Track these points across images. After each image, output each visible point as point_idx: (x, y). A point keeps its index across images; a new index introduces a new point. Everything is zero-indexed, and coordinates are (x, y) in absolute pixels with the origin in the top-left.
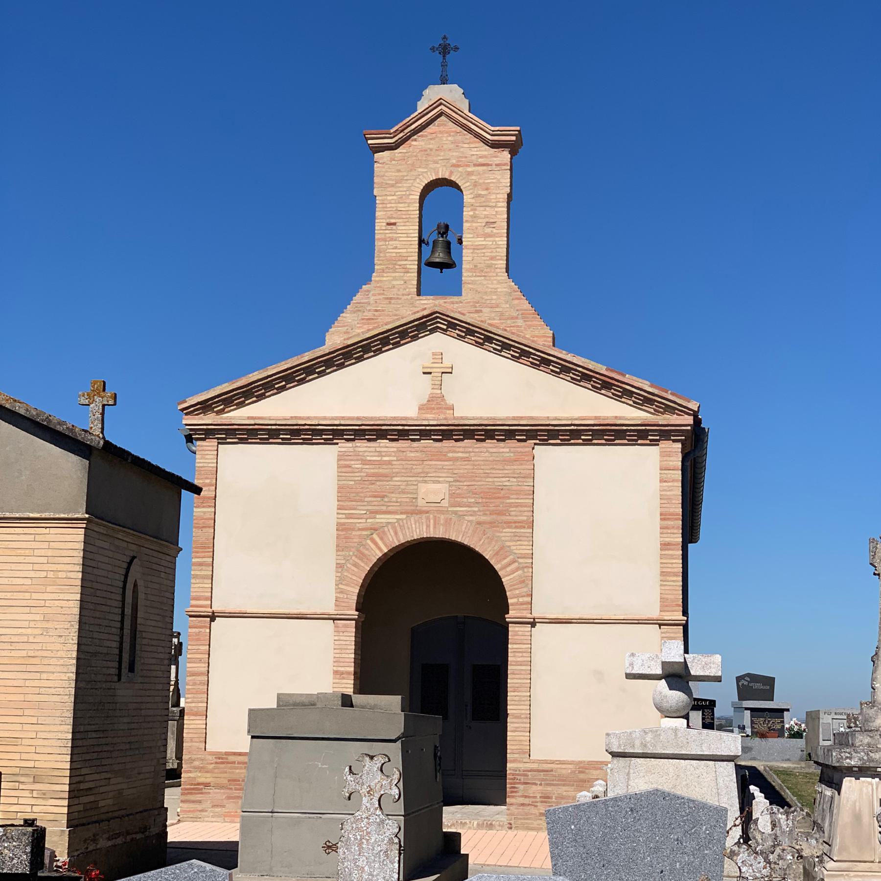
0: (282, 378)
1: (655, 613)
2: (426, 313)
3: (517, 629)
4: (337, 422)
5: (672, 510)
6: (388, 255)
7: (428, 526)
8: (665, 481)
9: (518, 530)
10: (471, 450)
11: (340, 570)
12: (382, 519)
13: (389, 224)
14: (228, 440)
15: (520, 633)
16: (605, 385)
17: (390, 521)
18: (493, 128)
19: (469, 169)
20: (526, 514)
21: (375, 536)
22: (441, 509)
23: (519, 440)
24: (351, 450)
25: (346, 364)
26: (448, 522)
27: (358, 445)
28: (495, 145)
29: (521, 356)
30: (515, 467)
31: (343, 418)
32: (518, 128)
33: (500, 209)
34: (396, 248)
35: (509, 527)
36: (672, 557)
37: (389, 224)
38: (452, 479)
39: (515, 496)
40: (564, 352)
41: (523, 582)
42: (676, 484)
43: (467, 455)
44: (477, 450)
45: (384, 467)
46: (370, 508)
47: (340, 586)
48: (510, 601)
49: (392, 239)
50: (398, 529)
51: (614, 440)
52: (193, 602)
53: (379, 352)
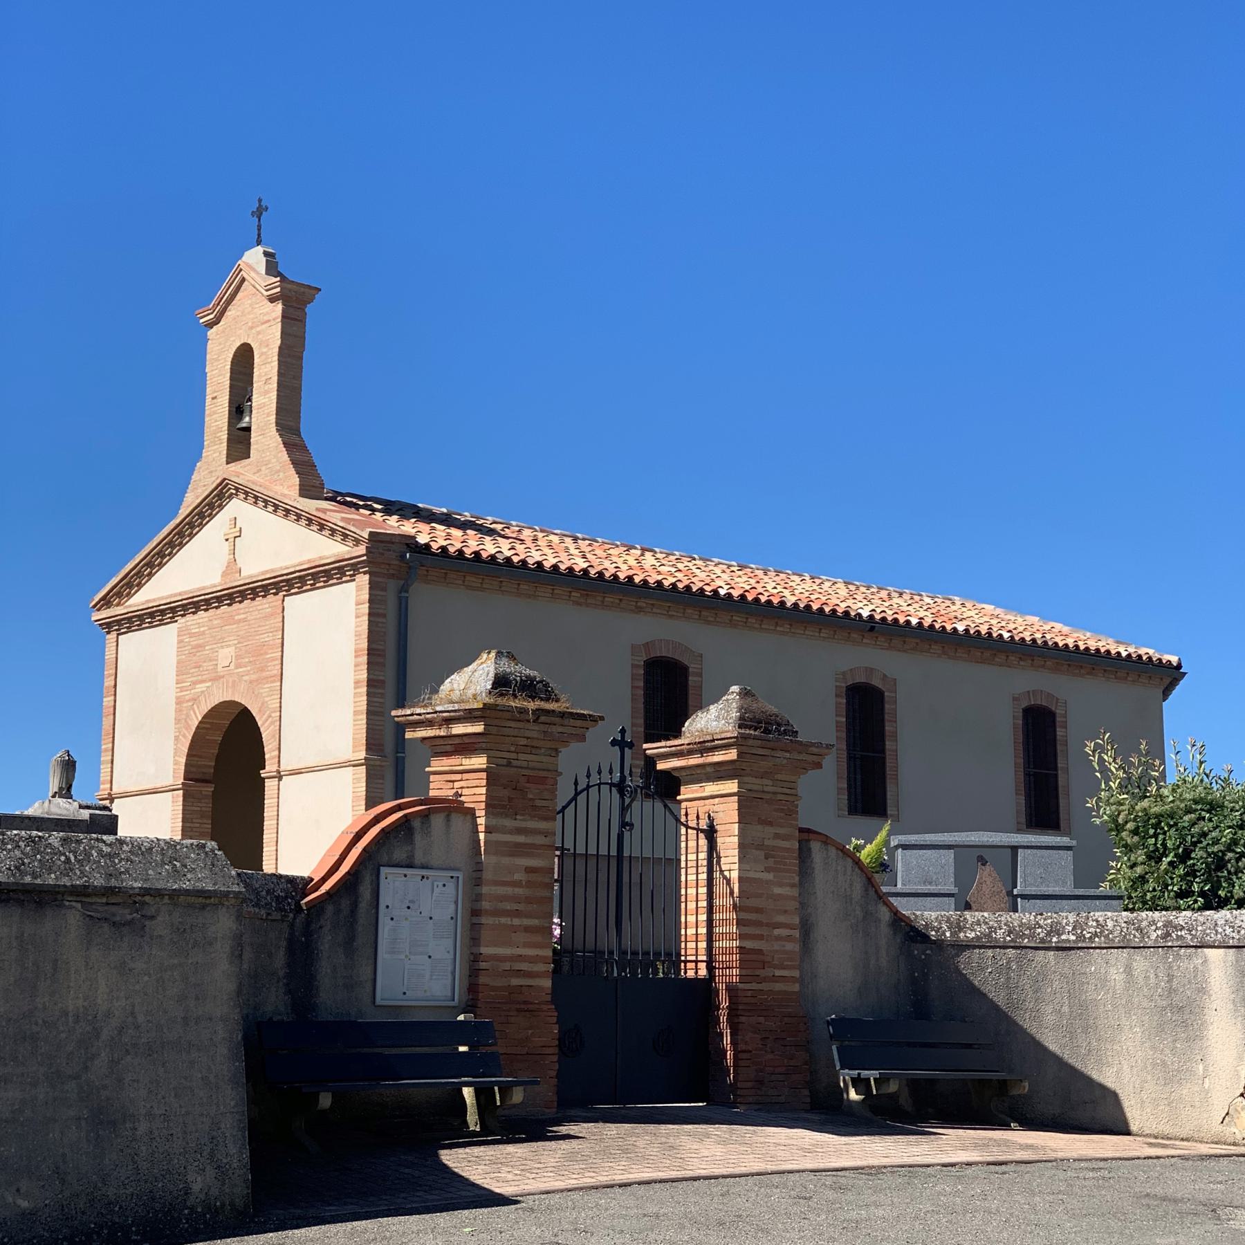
0: (147, 565)
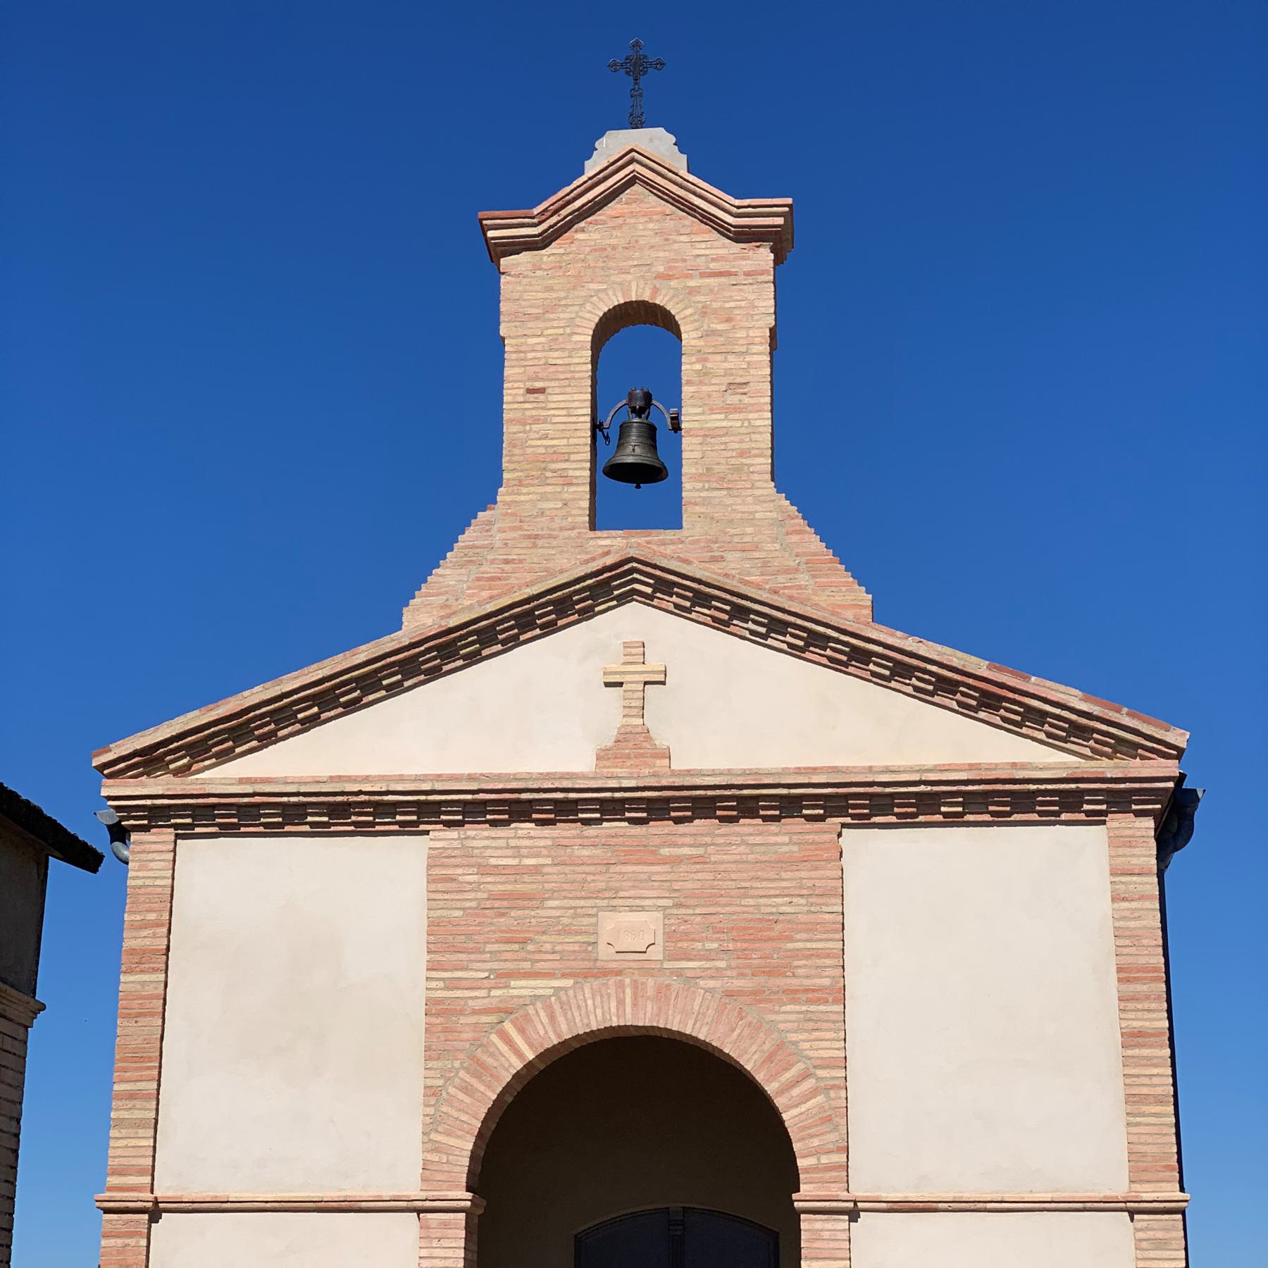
0: (313, 699)
1: (1118, 1186)
2: (609, 561)
3: (818, 1225)
4: (426, 786)
5: (1142, 961)
6: (529, 451)
7: (621, 1002)
8: (1125, 899)
9: (813, 1008)
10: (708, 839)
11: (433, 1100)
12: (522, 988)
13: (530, 391)
14: (198, 830)
15: (826, 1235)
16: (985, 701)
17: (541, 992)
18: (737, 202)
19: (692, 283)
20: (829, 972)
21: (508, 1026)
22: (647, 965)
23: (810, 818)
24: (456, 844)
25: (445, 668)
26: (662, 993)
27: (469, 833)
28: (743, 236)
29: (808, 645)
30: (803, 874)
31: (439, 777)
32: (789, 201)
33: (756, 358)
34: (546, 437)
35: (794, 1001)
36: (1150, 1061)
37: (530, 391)
38: (669, 903)
39: (804, 936)
40: (899, 633)
41: (829, 1119)
42: (1148, 904)
43: (701, 851)
44: (721, 840)
45: (526, 878)
46: (495, 965)
47: (434, 1136)
48: (801, 1163)
49: (537, 420)
50: (557, 1007)
51: (1009, 814)
52: (113, 1180)
53: (513, 643)
